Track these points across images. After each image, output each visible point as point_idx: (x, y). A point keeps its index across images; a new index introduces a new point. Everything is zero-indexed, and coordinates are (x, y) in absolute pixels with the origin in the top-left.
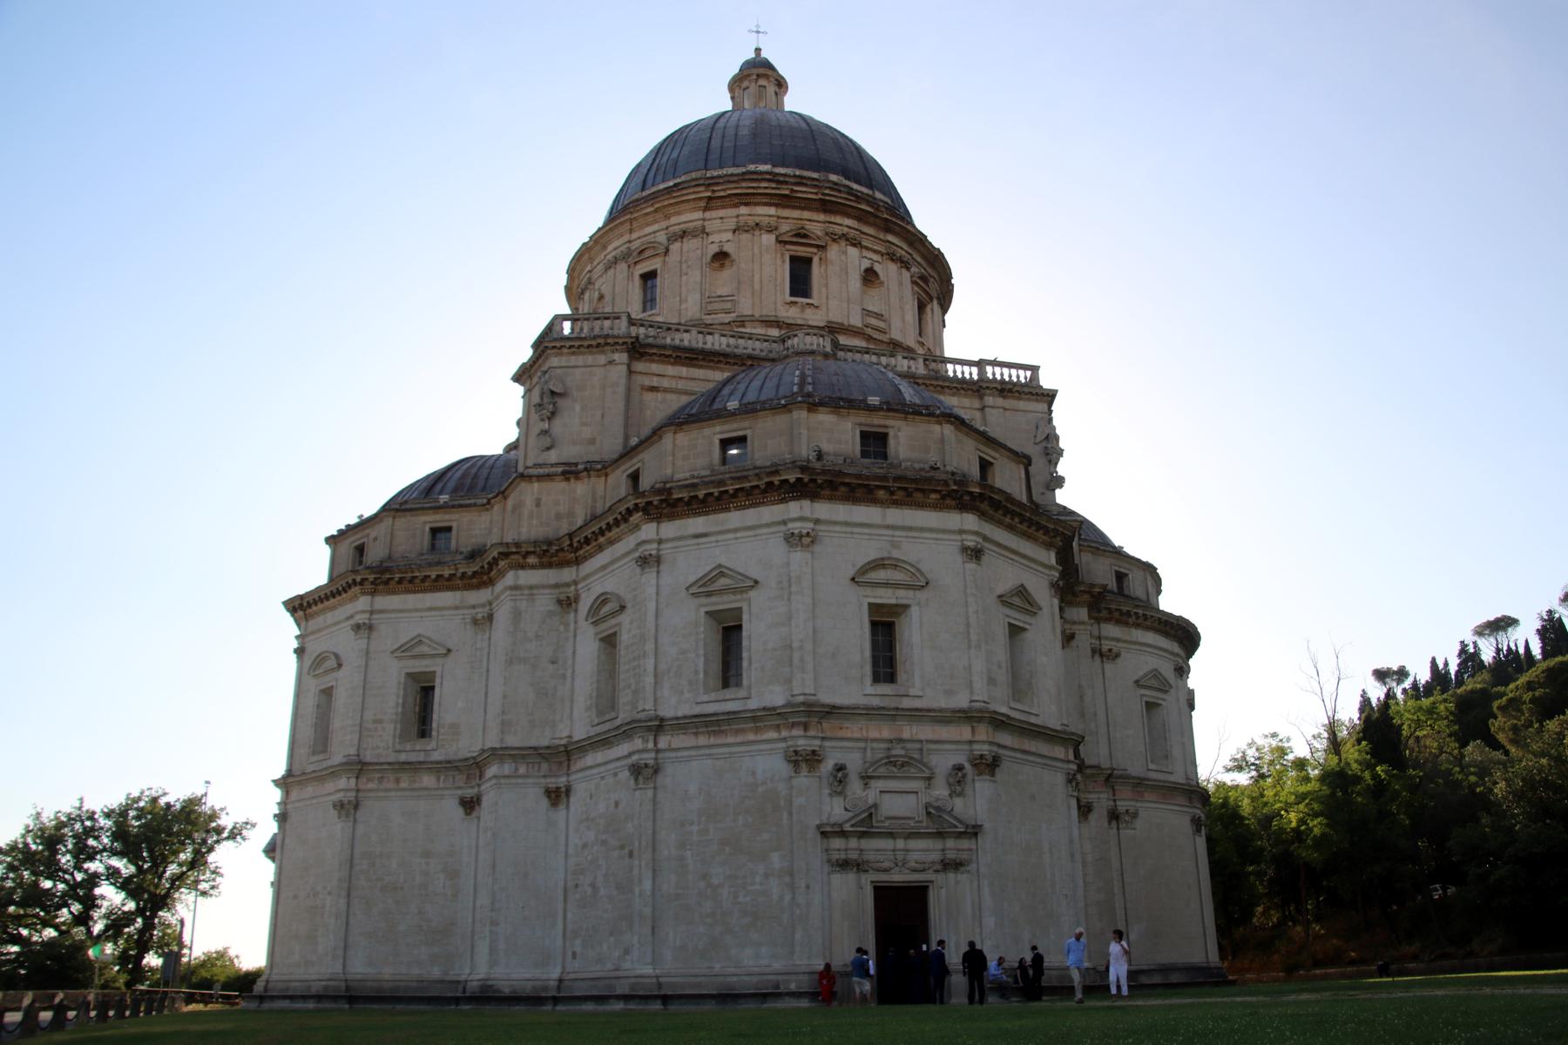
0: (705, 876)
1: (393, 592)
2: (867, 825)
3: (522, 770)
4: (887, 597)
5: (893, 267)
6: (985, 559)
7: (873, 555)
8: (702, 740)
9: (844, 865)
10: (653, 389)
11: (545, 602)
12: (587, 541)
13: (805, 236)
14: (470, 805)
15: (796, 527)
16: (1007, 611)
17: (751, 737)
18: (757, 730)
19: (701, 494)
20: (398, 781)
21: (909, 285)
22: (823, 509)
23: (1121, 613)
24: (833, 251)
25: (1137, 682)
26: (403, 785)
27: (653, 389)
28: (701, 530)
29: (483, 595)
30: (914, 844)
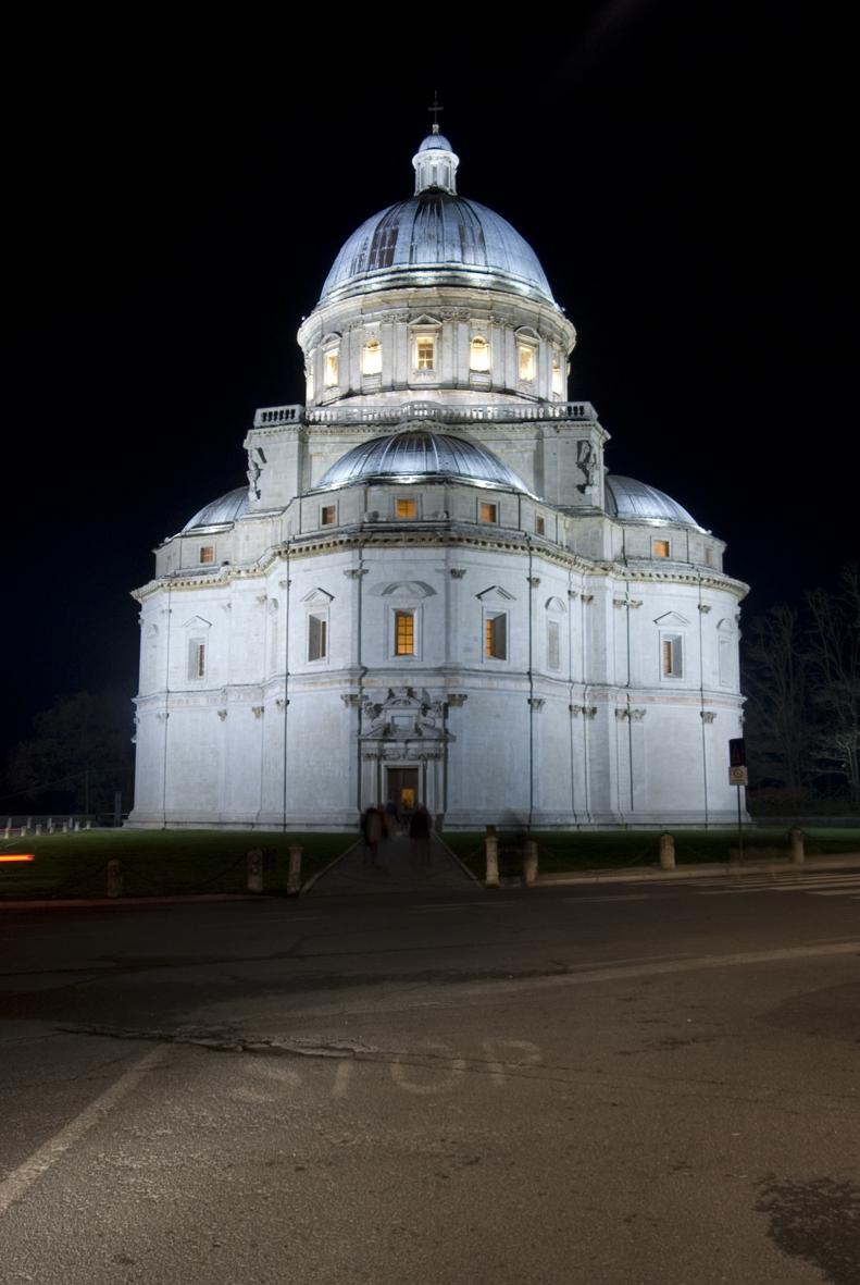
0: (308, 762)
1: (180, 590)
2: (387, 733)
3: (242, 698)
4: (403, 606)
5: (496, 333)
6: (465, 576)
7: (396, 579)
8: (307, 688)
9: (369, 756)
10: (319, 454)
11: (251, 600)
12: (265, 567)
13: (427, 323)
14: (223, 715)
15: (351, 567)
16: (485, 603)
17: (328, 686)
18: (331, 683)
19: (304, 547)
20: (187, 701)
21: (512, 341)
22: (366, 553)
23: (643, 575)
24: (447, 332)
25: (655, 621)
26: (191, 704)
27: (319, 454)
28: (308, 566)
29: (225, 592)
30: (410, 745)
